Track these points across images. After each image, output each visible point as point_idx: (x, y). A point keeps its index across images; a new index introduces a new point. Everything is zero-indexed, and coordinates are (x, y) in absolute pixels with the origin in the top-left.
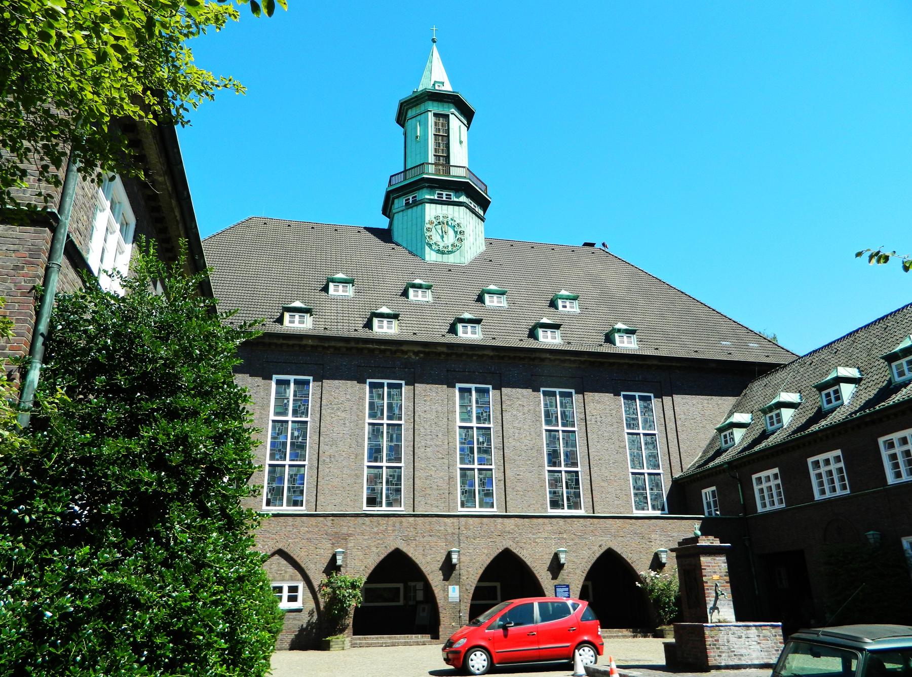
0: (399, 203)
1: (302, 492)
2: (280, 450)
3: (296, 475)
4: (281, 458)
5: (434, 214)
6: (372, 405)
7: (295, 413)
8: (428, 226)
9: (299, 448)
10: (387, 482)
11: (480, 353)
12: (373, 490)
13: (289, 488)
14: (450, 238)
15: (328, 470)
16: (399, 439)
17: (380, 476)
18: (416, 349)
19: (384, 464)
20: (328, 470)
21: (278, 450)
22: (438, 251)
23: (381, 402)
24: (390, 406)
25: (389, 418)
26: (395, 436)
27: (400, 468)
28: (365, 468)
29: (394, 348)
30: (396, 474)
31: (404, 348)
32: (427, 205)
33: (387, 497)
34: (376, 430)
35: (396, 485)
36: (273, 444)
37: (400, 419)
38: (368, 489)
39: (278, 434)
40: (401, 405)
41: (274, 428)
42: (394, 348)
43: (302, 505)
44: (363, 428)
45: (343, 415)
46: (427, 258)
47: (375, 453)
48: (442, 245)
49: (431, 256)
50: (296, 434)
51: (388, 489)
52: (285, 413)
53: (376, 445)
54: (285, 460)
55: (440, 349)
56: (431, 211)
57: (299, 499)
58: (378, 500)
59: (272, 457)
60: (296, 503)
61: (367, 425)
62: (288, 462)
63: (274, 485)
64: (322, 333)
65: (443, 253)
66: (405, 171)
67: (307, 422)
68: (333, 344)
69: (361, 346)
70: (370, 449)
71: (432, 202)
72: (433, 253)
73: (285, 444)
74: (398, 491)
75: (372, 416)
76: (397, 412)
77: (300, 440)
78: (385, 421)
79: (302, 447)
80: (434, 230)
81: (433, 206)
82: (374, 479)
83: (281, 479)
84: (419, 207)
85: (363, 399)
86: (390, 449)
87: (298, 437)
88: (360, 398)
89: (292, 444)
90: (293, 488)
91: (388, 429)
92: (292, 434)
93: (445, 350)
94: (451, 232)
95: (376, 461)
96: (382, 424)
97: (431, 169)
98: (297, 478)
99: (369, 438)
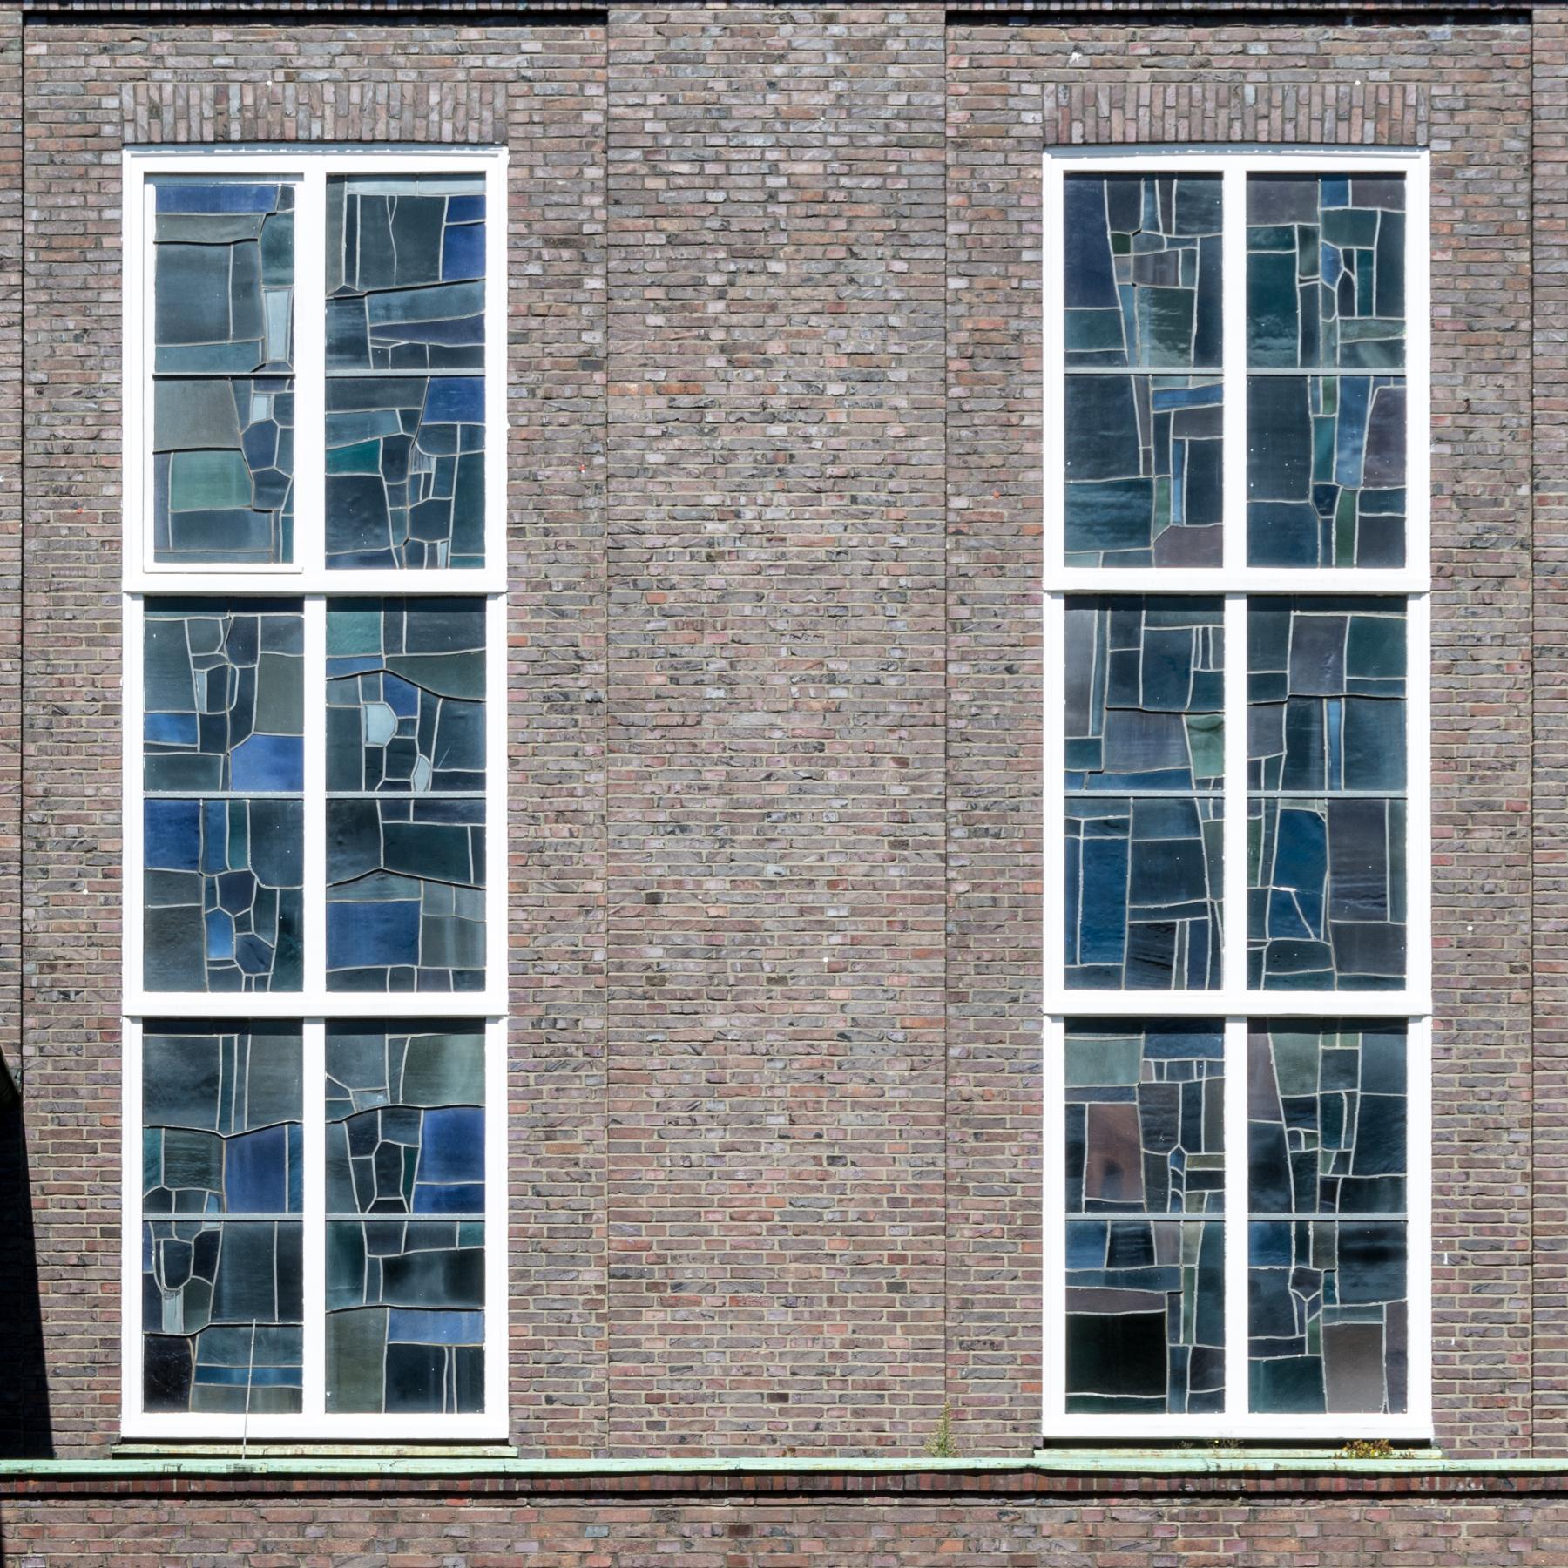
1: (465, 1275)
2: (236, 889)
3: (400, 1117)
4: (252, 955)
6: (1099, 413)
7: (356, 511)
9: (411, 844)
10: (1267, 1172)
12: (1135, 1246)
13: (344, 1244)
15: (694, 1071)
16: (1375, 752)
17: (1197, 1119)
19: (1235, 995)
20: (694, 1071)
21: (219, 886)
23: (1187, 372)
24: (1279, 417)
25: (1273, 541)
26: (1333, 718)
27: (1396, 1026)
28: (1054, 1038)
30: (1351, 1095)
33: (1269, 1313)
34: (1146, 666)
35: (1356, 1195)
36: (171, 830)
37: (1384, 543)
38: (1078, 1238)
39: (214, 734)
40: (1393, 408)
41: (165, 663)
43: (472, 1397)
44: (1016, 662)
45: (814, 528)
47: (1140, 898)
50: (379, 724)
51: (1267, 1243)
52: (254, 521)
53: (1148, 814)
54: (289, 973)
57: (437, 1333)
58: (1182, 1341)
59: (172, 951)
60: (417, 1379)
61: (1054, 615)
62: (315, 997)
63: (210, 1218)
67: (474, 603)
70: (1095, 867)
73: (275, 827)
74: (1379, 1252)
75: (1109, 525)
76: (1350, 470)
77: (421, 781)
78: (1236, 572)
79: (447, 849)
82: (1139, 1141)
83: (271, 1165)
85: (1017, 351)
86: (1290, 845)
87: (400, 756)
88: (979, 347)
89: (348, 825)
90: (384, 1236)
91: (1263, 643)
92: (343, 726)
95: (1152, 967)
96: (1213, 602)
98: (411, 1152)
99: (1079, 751)
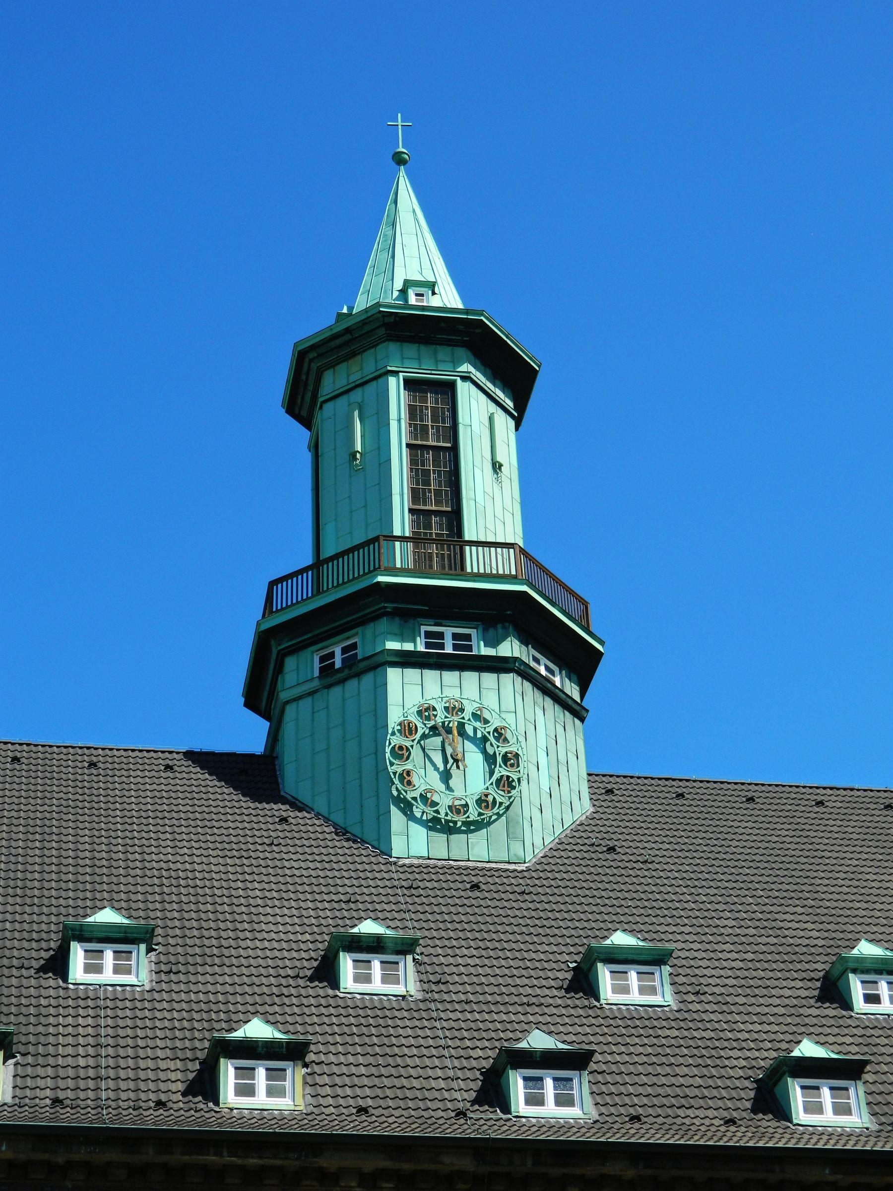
0: (300, 670)
5: (414, 699)
8: (397, 740)
11: (590, 1171)
14: (474, 778)
18: (371, 1163)
22: (435, 825)
29: (291, 1163)
31: (329, 1162)
32: (393, 675)
42: (291, 1163)
46: (398, 847)
48: (444, 801)
49: (411, 842)
55: (451, 1162)
56: (407, 693)
64: (45, 1117)
65: (446, 828)
66: (318, 564)
68: (80, 1154)
69: (177, 1158)
71: (407, 660)
72: (419, 833)
80: (416, 752)
81: (413, 674)
84: (368, 679)
93: (466, 1163)
94: (474, 759)
97: (401, 555)
